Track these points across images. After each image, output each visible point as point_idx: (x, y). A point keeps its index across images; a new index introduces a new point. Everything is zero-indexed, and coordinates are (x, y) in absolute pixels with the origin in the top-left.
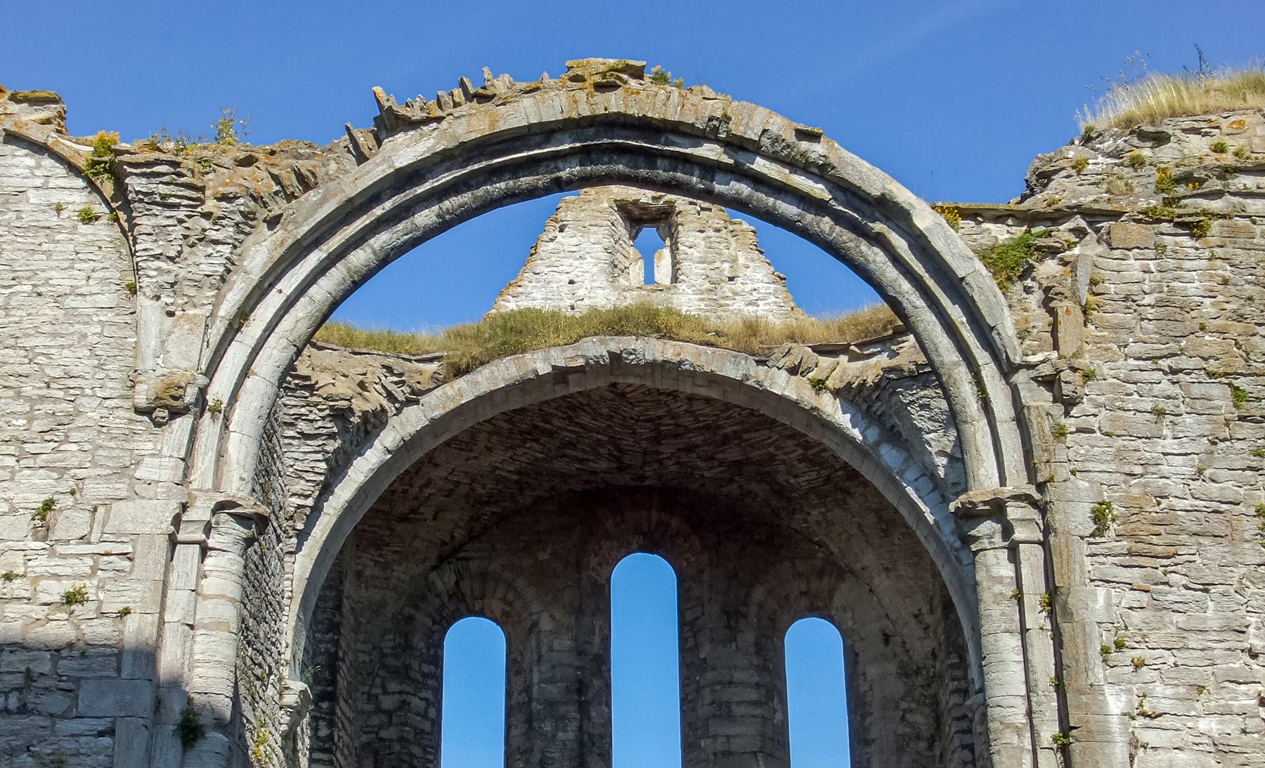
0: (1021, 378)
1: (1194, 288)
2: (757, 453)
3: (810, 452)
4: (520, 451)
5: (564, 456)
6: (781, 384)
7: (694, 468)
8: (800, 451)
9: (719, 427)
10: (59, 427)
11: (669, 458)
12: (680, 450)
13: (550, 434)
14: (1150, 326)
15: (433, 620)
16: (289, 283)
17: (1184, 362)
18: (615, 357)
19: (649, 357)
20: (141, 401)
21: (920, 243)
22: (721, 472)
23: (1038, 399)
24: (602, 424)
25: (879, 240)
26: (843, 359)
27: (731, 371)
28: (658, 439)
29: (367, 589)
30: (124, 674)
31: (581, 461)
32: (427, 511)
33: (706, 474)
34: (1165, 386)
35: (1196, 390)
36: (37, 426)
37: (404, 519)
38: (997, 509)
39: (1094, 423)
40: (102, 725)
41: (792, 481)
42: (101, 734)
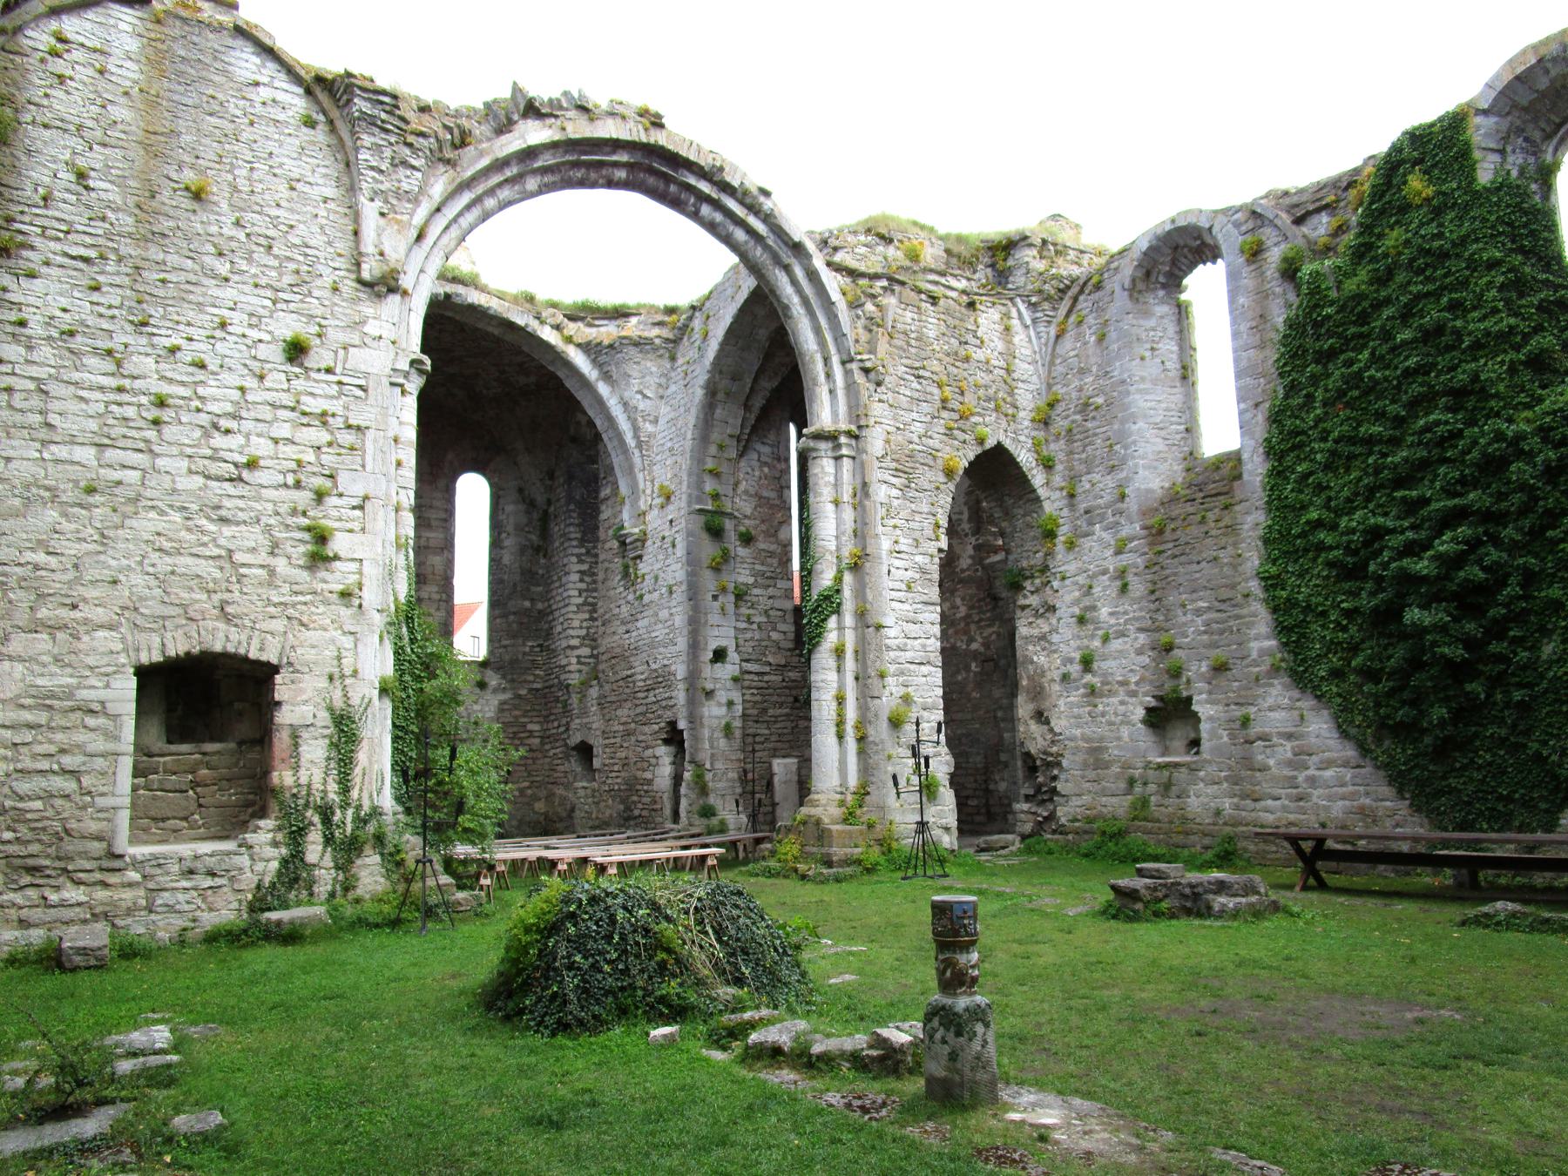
0: (854, 366)
1: (932, 334)
6: (548, 335)
10: (301, 283)
14: (913, 350)
16: (450, 212)
17: (921, 372)
18: (448, 296)
19: (470, 300)
20: (366, 275)
21: (813, 276)
23: (859, 378)
25: (787, 269)
26: (580, 324)
27: (520, 321)
30: (368, 468)
34: (915, 385)
35: (929, 389)
36: (288, 279)
38: (832, 437)
39: (884, 397)
40: (355, 502)
42: (354, 508)
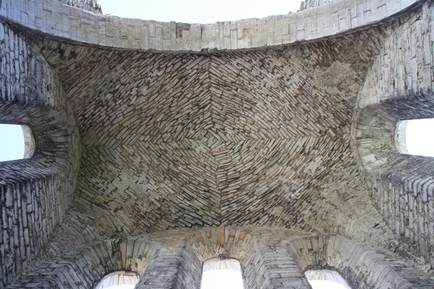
2: (274, 183)
3: (299, 171)
4: (162, 185)
5: (184, 192)
7: (246, 204)
8: (294, 173)
9: (255, 169)
11: (232, 197)
12: (238, 189)
13: (177, 175)
15: (101, 262)
22: (259, 204)
24: (200, 169)
28: (228, 182)
29: (69, 226)
31: (191, 198)
32: (113, 206)
33: (251, 208)
37: (99, 205)
41: (293, 195)
